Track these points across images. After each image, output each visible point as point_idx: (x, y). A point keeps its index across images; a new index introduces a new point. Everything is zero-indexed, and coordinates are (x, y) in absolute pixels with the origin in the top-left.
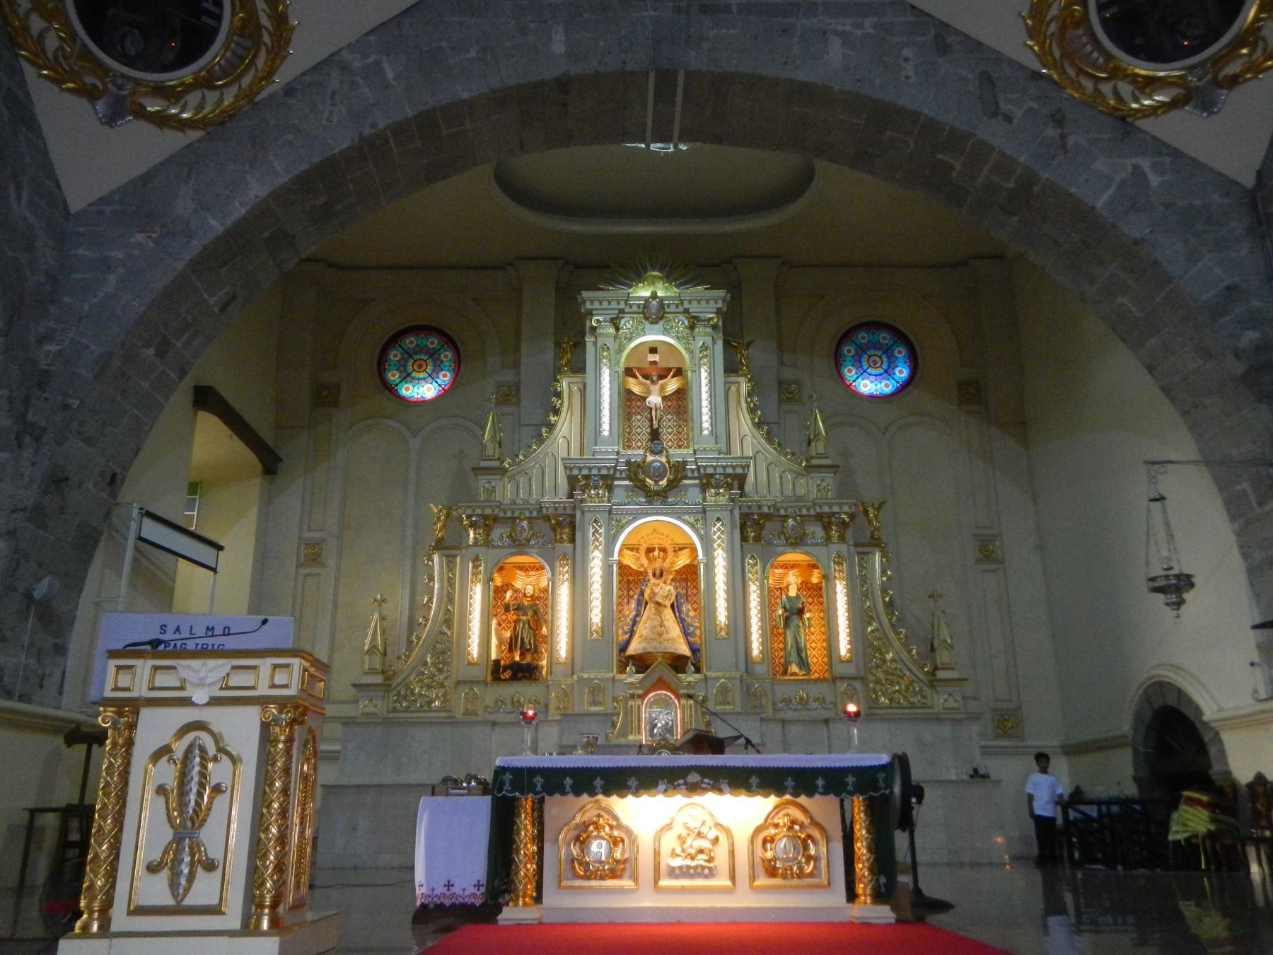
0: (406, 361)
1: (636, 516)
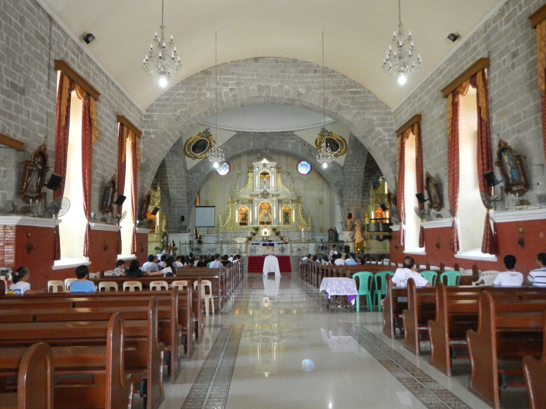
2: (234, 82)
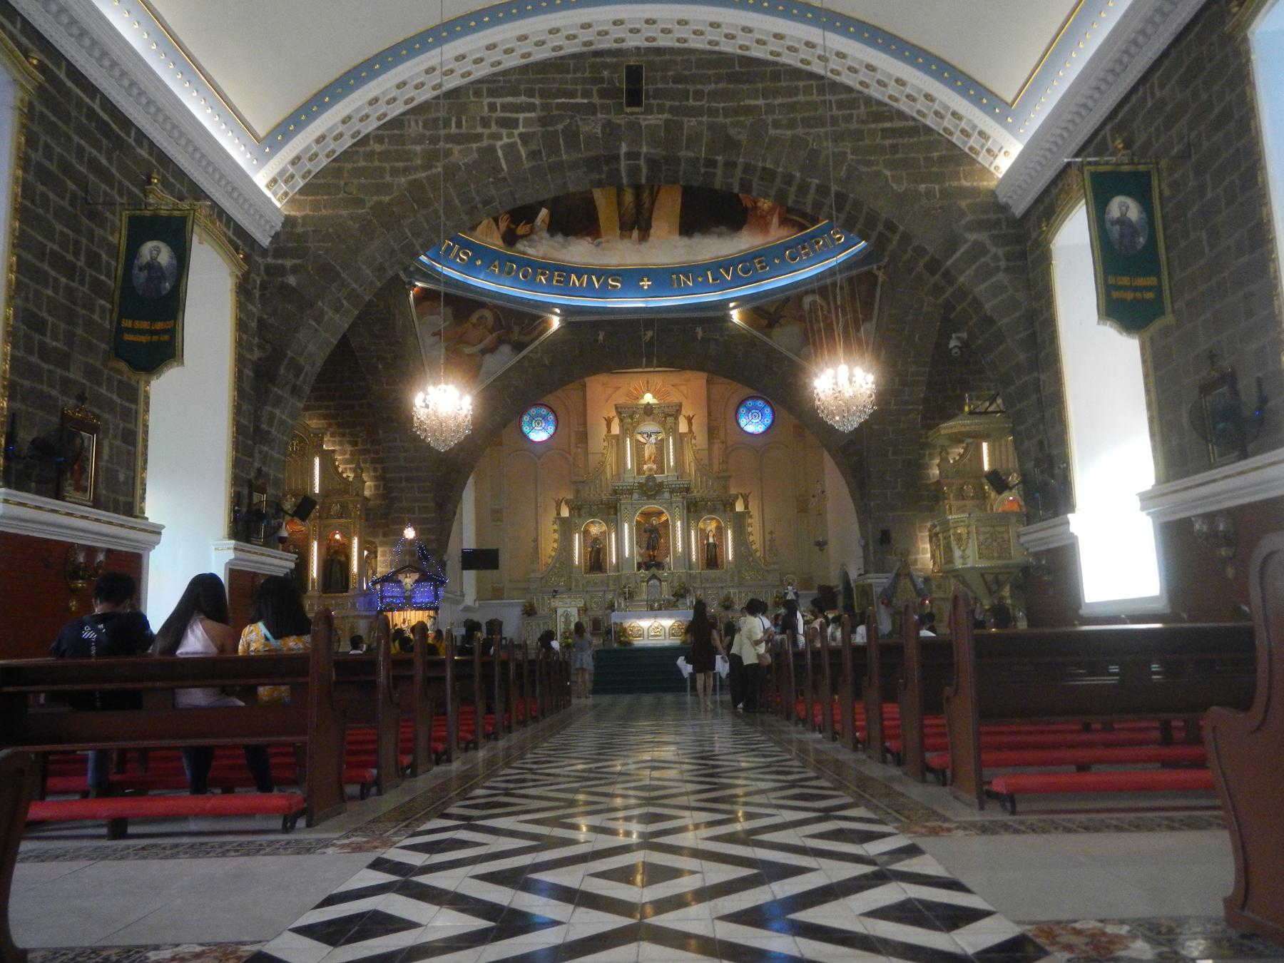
1: (643, 505)
2: (533, 115)
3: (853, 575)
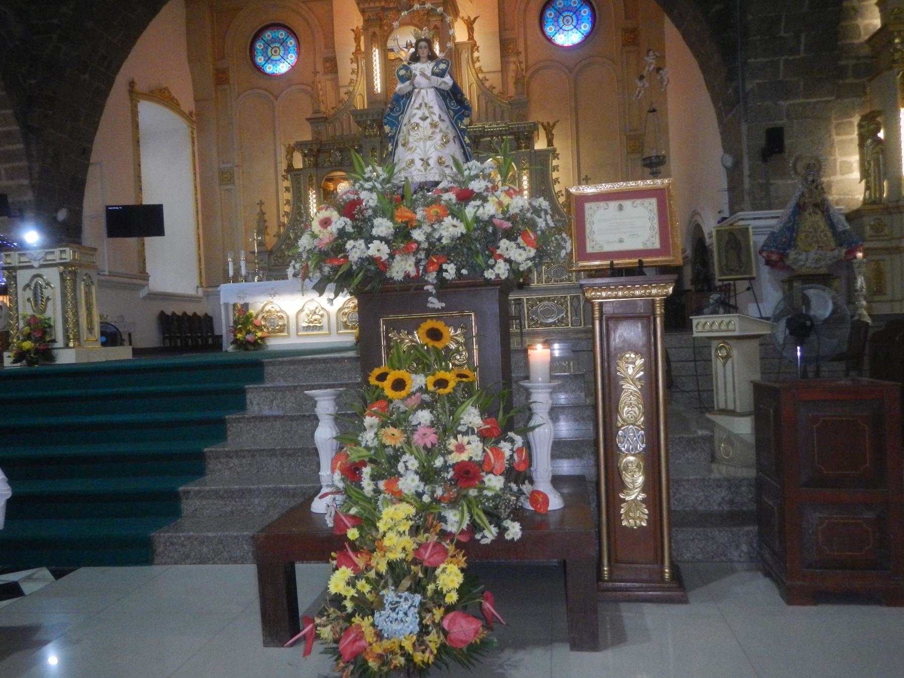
0: (267, 49)
3: (710, 226)
